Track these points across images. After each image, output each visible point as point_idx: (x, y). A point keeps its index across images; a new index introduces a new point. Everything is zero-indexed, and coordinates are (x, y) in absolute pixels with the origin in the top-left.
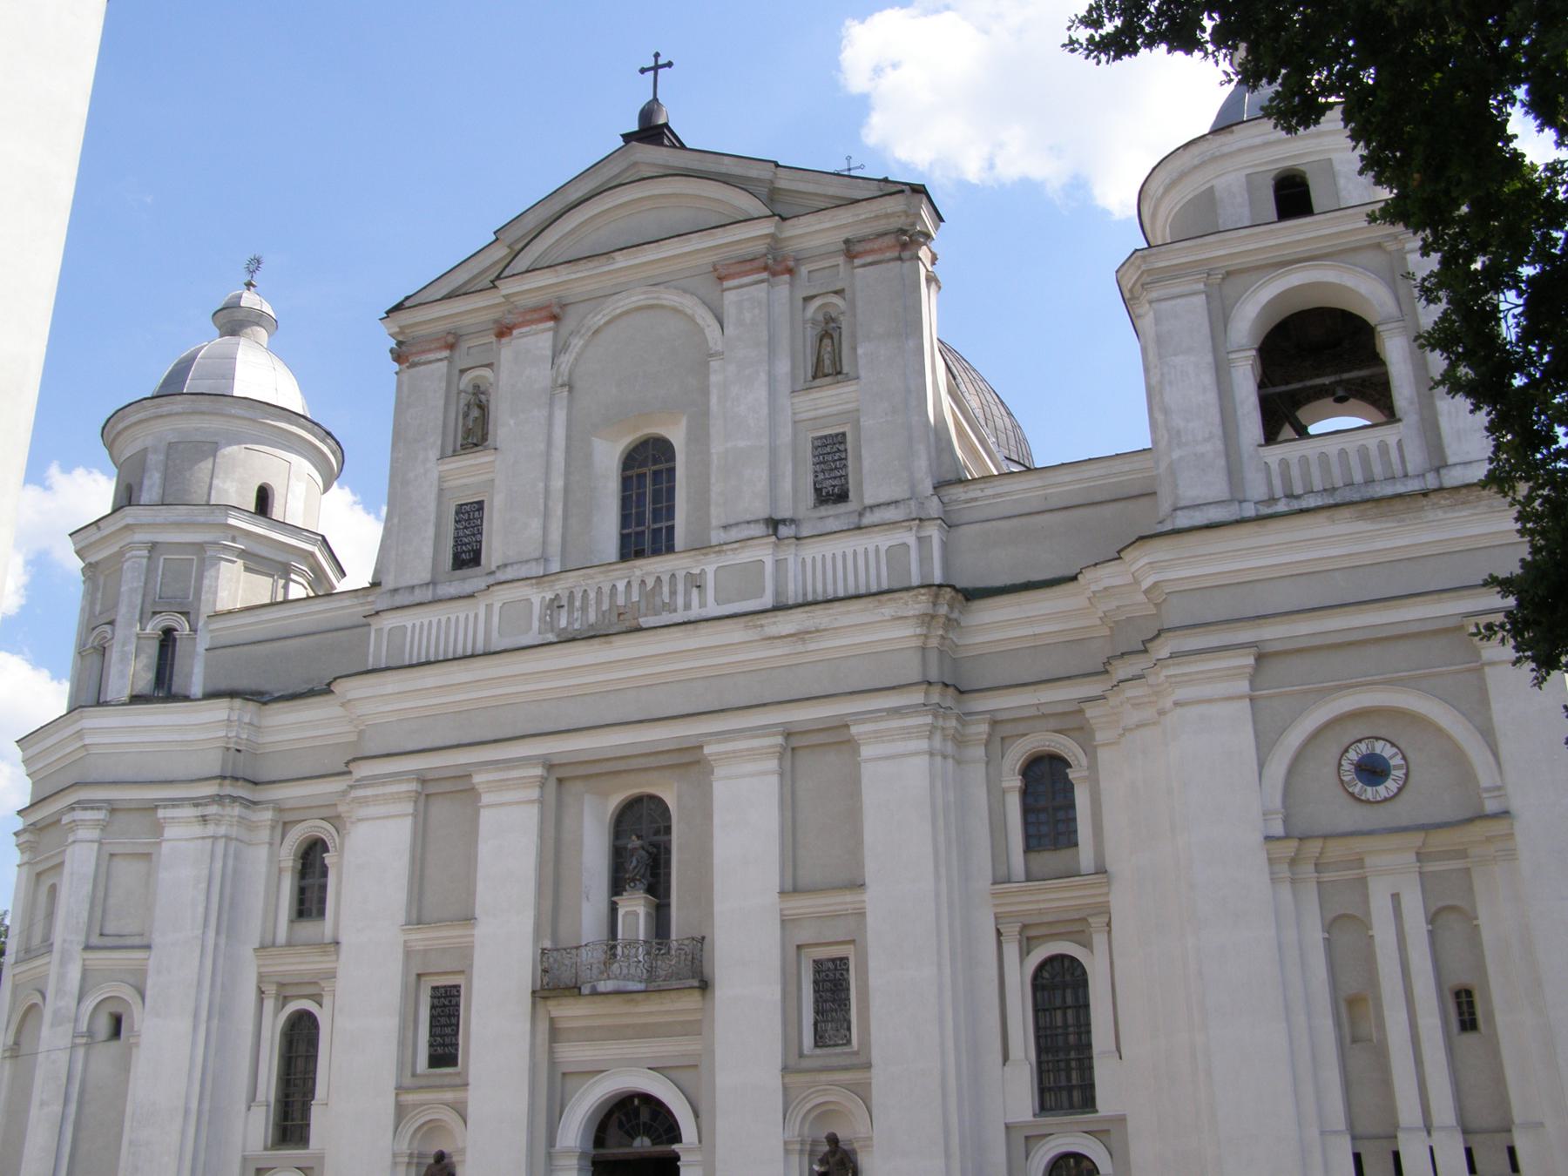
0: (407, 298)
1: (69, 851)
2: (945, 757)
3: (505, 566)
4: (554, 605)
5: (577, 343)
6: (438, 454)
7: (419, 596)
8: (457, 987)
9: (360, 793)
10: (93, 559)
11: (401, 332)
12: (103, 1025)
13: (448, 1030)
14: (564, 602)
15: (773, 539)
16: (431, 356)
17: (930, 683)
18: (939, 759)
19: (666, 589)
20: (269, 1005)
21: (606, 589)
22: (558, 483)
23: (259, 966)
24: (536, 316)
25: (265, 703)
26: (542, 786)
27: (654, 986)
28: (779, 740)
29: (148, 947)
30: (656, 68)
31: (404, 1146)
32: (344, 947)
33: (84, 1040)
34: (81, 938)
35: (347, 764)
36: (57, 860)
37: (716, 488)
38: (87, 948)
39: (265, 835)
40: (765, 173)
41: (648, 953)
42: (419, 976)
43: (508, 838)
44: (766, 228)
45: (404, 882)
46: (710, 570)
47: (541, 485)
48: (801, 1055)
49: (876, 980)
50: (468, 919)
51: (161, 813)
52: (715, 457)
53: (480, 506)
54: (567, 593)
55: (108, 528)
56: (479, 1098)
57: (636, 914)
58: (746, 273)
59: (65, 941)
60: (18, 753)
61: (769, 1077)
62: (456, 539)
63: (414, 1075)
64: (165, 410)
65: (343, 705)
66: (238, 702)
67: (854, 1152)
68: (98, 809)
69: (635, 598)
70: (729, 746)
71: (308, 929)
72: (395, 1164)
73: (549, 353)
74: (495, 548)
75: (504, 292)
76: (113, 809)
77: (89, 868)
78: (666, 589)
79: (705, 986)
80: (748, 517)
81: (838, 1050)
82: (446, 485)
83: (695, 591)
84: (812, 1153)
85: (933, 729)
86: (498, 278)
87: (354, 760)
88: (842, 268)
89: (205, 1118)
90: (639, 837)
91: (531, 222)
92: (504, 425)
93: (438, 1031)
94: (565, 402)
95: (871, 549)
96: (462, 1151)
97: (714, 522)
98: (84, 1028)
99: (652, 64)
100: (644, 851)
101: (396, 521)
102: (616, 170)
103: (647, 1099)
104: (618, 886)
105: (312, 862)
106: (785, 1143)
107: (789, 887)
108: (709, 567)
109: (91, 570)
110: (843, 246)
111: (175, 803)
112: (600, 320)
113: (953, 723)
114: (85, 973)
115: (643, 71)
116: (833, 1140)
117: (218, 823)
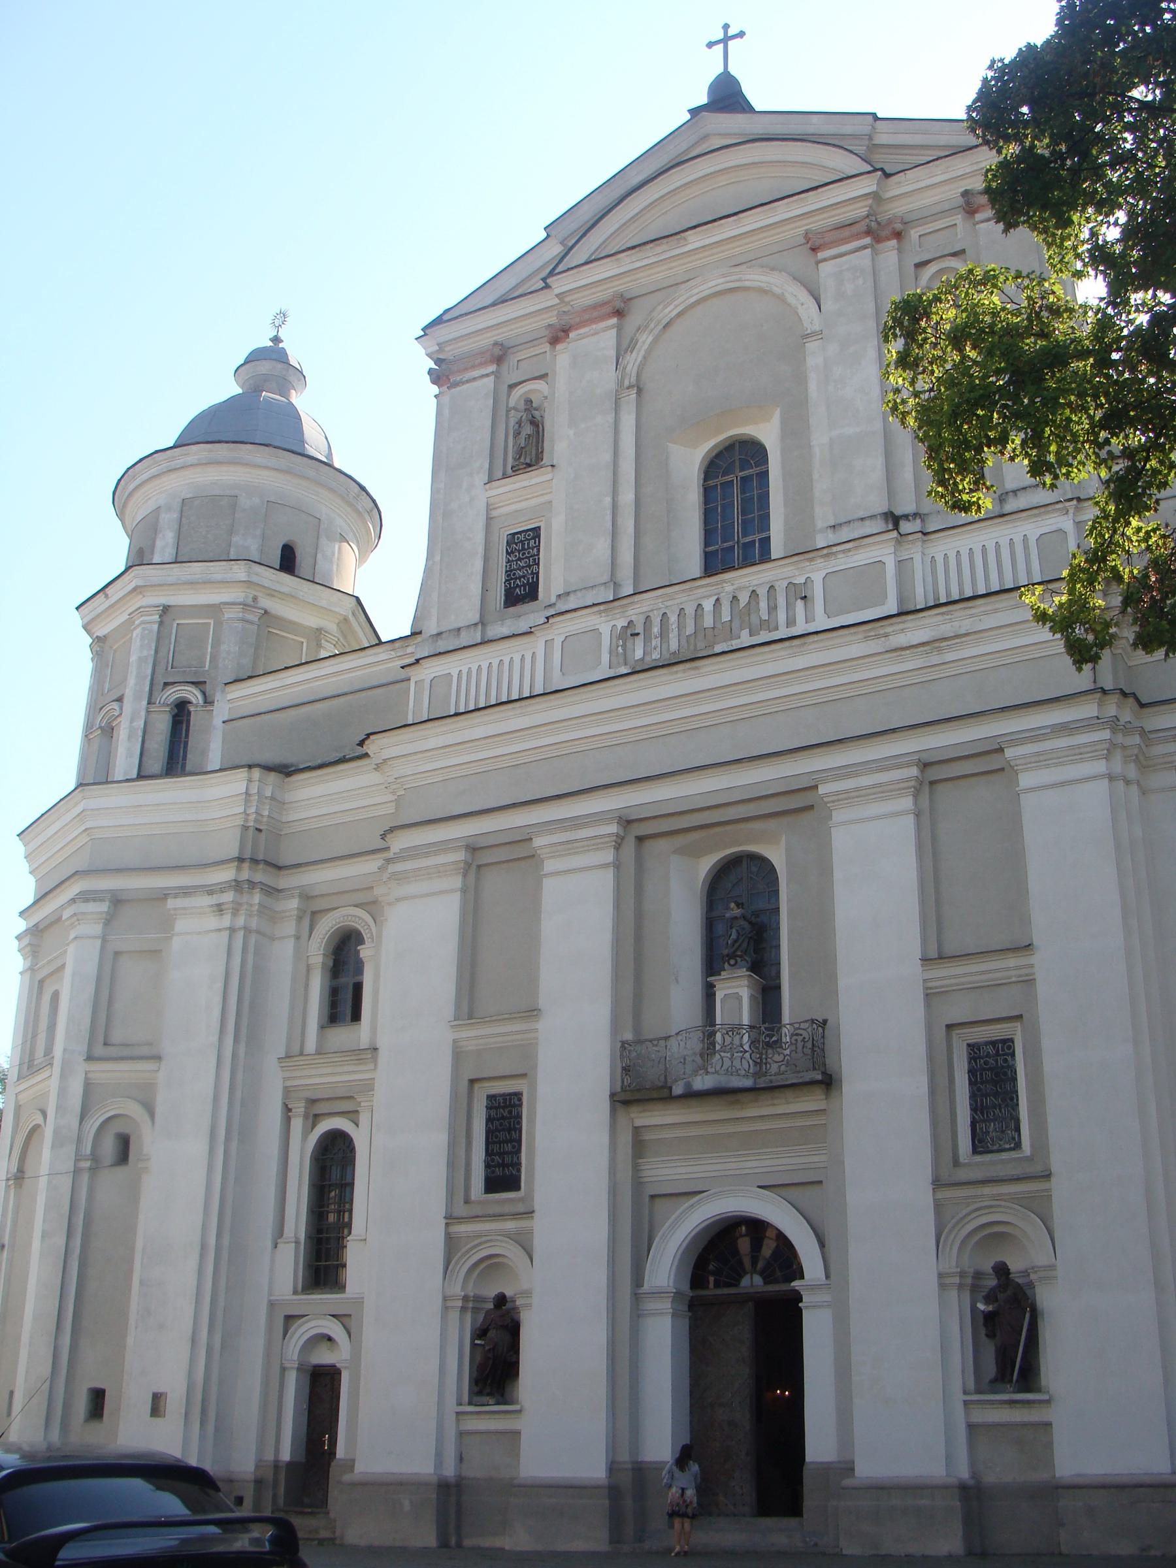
0: (447, 311)
1: (71, 950)
2: (1128, 782)
3: (568, 594)
4: (629, 633)
5: (645, 340)
6: (486, 480)
7: (465, 639)
8: (518, 1095)
9: (399, 867)
10: (100, 633)
11: (441, 350)
12: (109, 1147)
13: (508, 1147)
14: (639, 629)
15: (895, 534)
16: (476, 373)
17: (1104, 692)
18: (1121, 785)
19: (763, 605)
20: (297, 1124)
21: (690, 610)
22: (627, 496)
23: (285, 1079)
24: (595, 314)
25: (289, 774)
26: (617, 848)
27: (764, 1089)
28: (914, 771)
29: (158, 1058)
30: (726, 40)
31: (457, 1290)
32: (383, 1056)
33: (88, 1164)
34: (84, 1048)
35: (383, 837)
36: (59, 963)
37: (821, 485)
38: (90, 1058)
39: (289, 928)
40: (864, 128)
41: (753, 1043)
42: (472, 1082)
43: (576, 912)
44: (867, 185)
45: (452, 970)
46: (817, 578)
47: (608, 500)
48: (956, 1163)
49: (1051, 1064)
50: (532, 1013)
51: (171, 903)
52: (817, 451)
53: (537, 530)
54: (642, 619)
55: (115, 593)
56: (545, 1229)
57: (739, 998)
58: (845, 241)
59: (65, 1050)
60: (19, 848)
61: (919, 1195)
62: (509, 573)
63: (467, 1201)
64: (178, 463)
65: (378, 767)
66: (256, 773)
67: (1031, 1285)
68: (102, 900)
69: (726, 617)
70: (850, 784)
71: (341, 1036)
72: (446, 1309)
73: (613, 353)
74: (554, 576)
75: (557, 291)
76: (117, 901)
77: (91, 968)
78: (763, 605)
79: (828, 1082)
80: (861, 514)
81: (1004, 1156)
82: (494, 513)
83: (800, 604)
84: (974, 1289)
85: (1112, 747)
86: (552, 273)
87: (392, 830)
88: (959, 229)
89: (225, 1255)
90: (738, 905)
91: (586, 214)
92: (561, 440)
93: (496, 1148)
94: (633, 407)
95: (1018, 539)
96: (528, 1293)
97: (820, 524)
98: (88, 1150)
99: (721, 36)
100: (743, 921)
101: (437, 558)
102: (684, 146)
103: (757, 1227)
104: (712, 965)
105: (344, 955)
106: (941, 1276)
107: (933, 954)
108: (816, 573)
109: (100, 645)
110: (961, 201)
111: (186, 892)
112: (671, 311)
113: (1137, 739)
114: (88, 1087)
115: (710, 45)
116: (1002, 1270)
117: (235, 912)
